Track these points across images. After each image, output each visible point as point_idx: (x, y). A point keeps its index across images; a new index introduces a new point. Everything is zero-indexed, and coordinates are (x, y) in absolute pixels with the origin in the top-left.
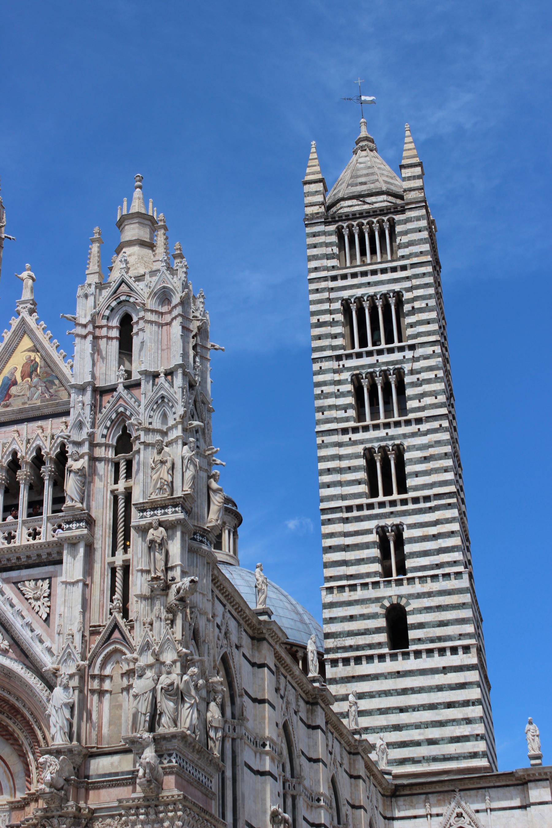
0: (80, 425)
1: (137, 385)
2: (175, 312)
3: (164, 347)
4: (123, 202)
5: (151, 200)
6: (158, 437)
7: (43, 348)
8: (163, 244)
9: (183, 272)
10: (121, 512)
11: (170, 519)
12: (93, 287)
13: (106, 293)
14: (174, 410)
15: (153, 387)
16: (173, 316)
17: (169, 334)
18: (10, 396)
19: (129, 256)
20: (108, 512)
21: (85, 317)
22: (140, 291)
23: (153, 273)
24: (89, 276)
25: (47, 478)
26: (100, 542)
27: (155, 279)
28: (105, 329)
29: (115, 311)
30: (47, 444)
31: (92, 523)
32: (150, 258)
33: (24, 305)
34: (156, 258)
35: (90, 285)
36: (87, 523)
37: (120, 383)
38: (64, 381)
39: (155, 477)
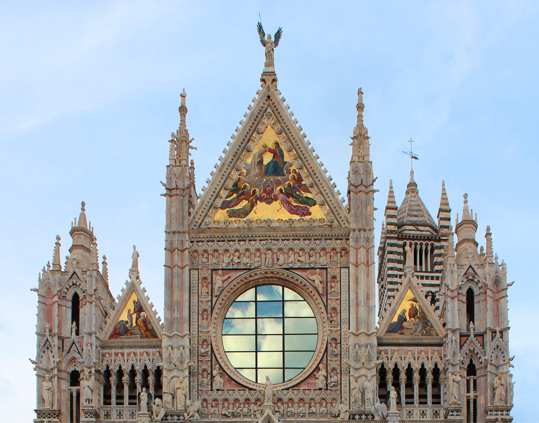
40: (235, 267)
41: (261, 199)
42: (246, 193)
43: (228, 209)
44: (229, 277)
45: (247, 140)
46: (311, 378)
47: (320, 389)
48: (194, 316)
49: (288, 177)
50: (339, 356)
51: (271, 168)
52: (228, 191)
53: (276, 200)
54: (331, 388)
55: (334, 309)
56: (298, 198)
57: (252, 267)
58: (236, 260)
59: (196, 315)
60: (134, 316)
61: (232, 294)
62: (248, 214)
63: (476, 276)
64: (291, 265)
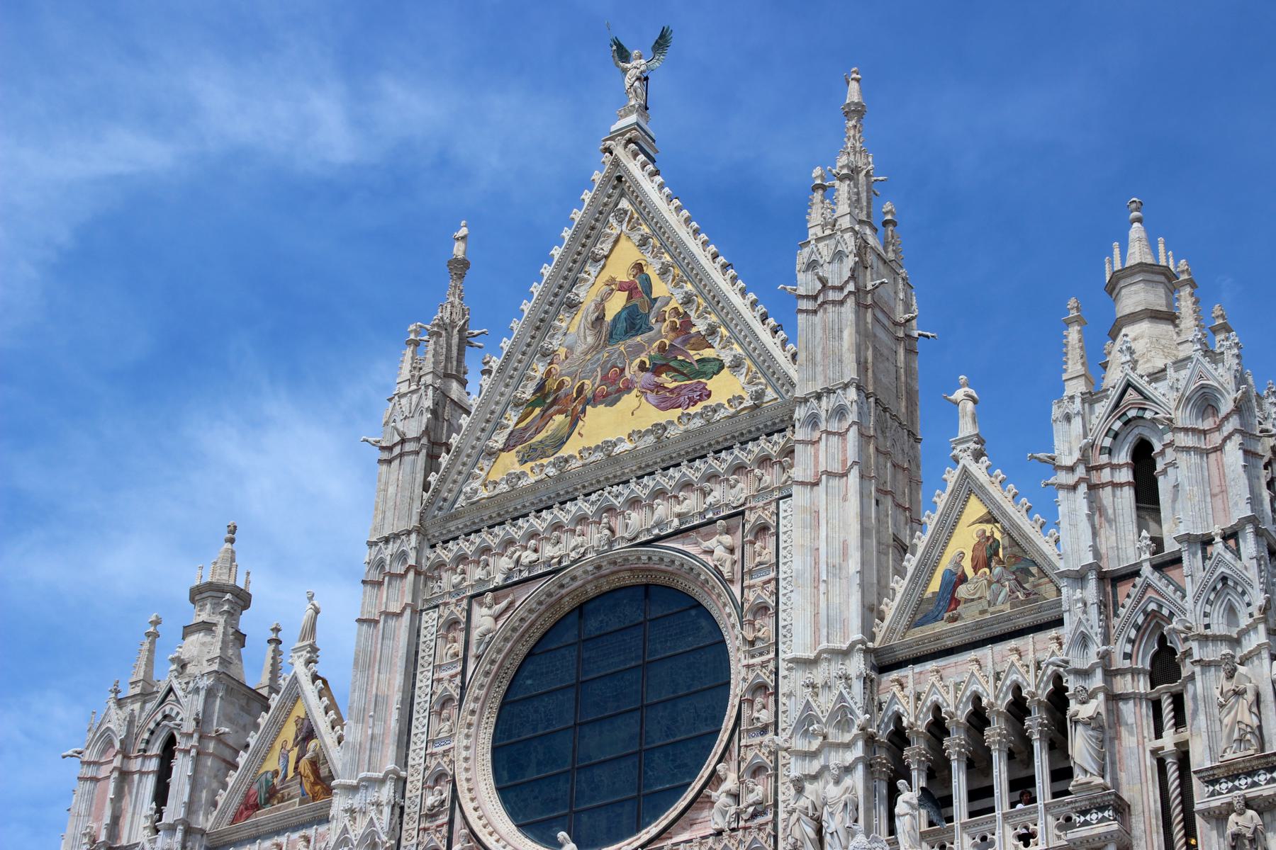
0: (1083, 641)
1: (1176, 561)
2: (1228, 427)
3: (1217, 490)
4: (1112, 250)
5: (1161, 239)
6: (1225, 650)
7: (1004, 514)
8: (1191, 312)
9: (1233, 355)
10: (1174, 787)
11: (1265, 793)
12: (1078, 401)
13: (1102, 408)
14: (1246, 598)
15: (1204, 562)
16: (1226, 434)
17: (1221, 466)
18: (958, 602)
19: (1135, 339)
20: (1151, 788)
21: (1070, 453)
22: (1162, 398)
23: (1180, 363)
24: (1069, 382)
25: (1036, 736)
26: (1143, 843)
27: (1185, 373)
28: (1107, 471)
29: (1120, 437)
30: (1031, 678)
31: (1124, 810)
32: (1172, 339)
33: (965, 446)
34: (1183, 338)
35: (1072, 398)
36: (1116, 810)
37: (1145, 560)
38: (1046, 568)
39: (1227, 720)
40: (525, 574)
41: (595, 400)
42: (563, 396)
43: (519, 447)
44: (511, 603)
45: (567, 285)
46: (700, 805)
47: (719, 833)
48: (421, 719)
49: (660, 331)
50: (772, 728)
51: (622, 325)
52: (521, 407)
53: (628, 389)
54: (748, 824)
55: (762, 609)
56: (681, 369)
57: (564, 564)
58: (528, 557)
59: (424, 717)
60: (293, 756)
61: (517, 641)
62: (564, 443)
63: (1148, 405)
64: (656, 531)
